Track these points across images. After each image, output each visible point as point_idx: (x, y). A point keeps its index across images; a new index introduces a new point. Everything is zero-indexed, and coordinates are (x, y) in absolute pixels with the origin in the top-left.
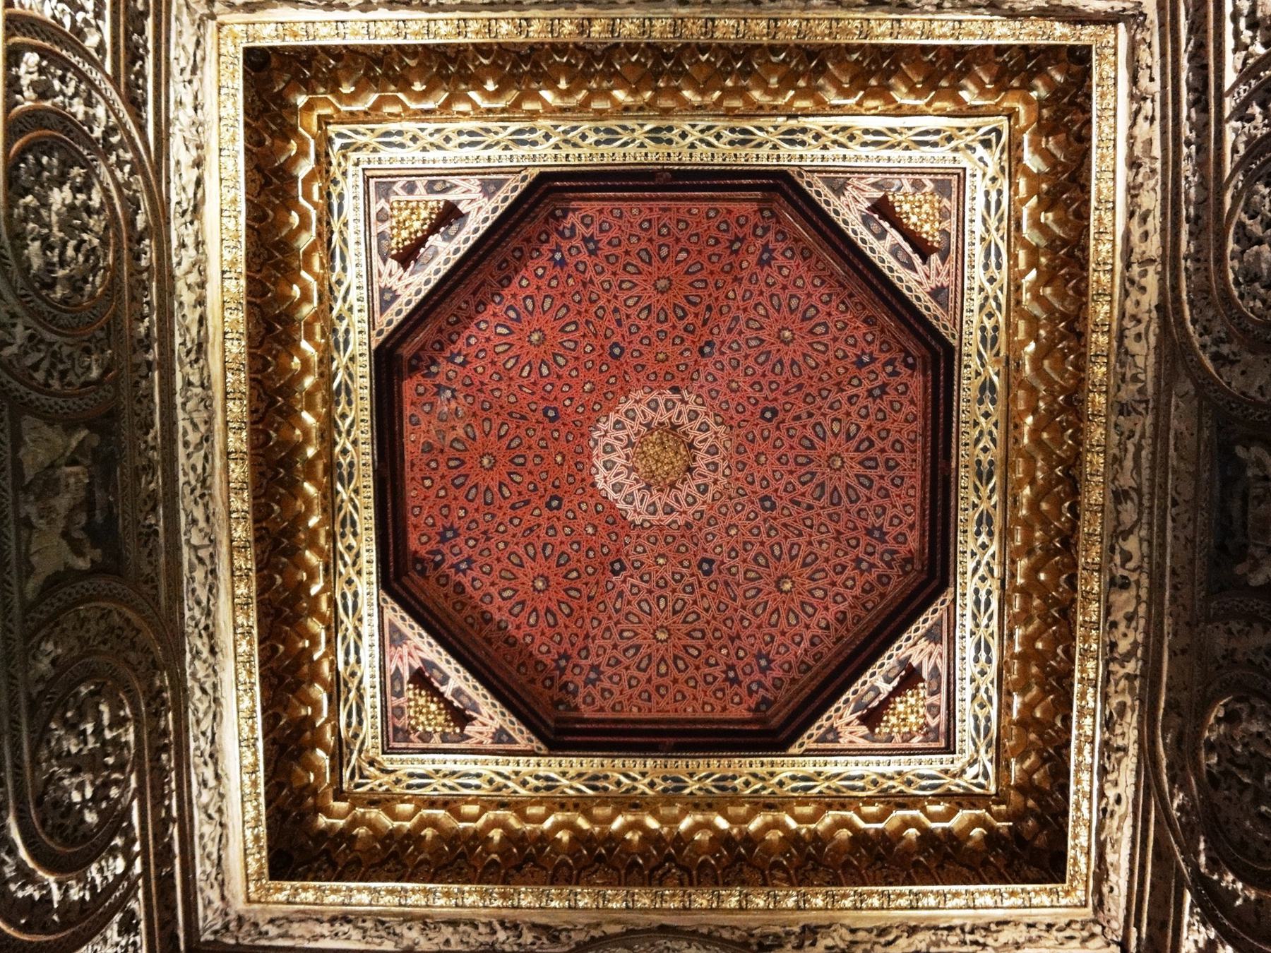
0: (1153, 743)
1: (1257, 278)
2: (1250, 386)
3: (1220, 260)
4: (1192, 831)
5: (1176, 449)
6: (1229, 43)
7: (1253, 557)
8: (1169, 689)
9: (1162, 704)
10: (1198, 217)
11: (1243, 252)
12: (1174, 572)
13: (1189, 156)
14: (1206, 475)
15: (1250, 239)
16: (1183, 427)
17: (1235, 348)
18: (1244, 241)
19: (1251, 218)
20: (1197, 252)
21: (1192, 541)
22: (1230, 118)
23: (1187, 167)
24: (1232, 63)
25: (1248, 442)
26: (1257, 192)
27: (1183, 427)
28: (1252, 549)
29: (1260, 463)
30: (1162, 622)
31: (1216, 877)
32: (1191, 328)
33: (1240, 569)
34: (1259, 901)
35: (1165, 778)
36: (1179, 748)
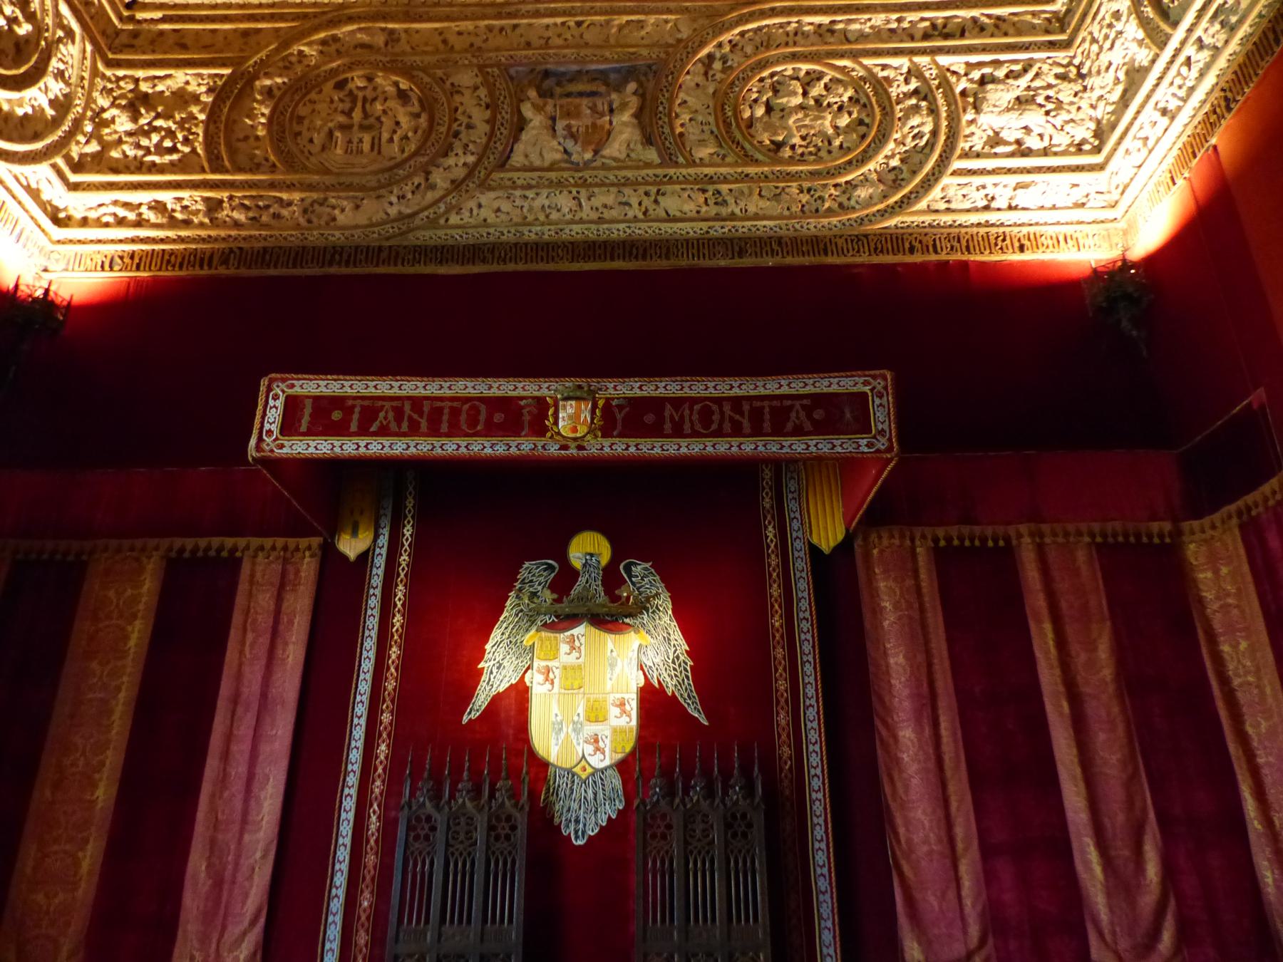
0: (351, 19)
1: (776, 92)
2: (687, 94)
3: (794, 57)
4: (286, 68)
5: (627, 22)
6: (974, 59)
7: (545, 105)
8: (406, 31)
9: (390, 26)
10: (832, 32)
11: (797, 79)
12: (515, 27)
13: (888, 22)
14: (607, 54)
15: (808, 84)
16: (649, 29)
17: (719, 76)
18: (808, 79)
19: (826, 86)
20: (803, 33)
21: (547, 45)
22: (911, 60)
23: (878, 19)
24: (956, 62)
25: (641, 94)
26: (846, 90)
27: (649, 29)
28: (550, 101)
29: (624, 106)
30: (466, 18)
31: (259, 97)
32: (737, 31)
33: (532, 93)
34: (257, 138)
35: (322, 35)
36: (356, 47)
